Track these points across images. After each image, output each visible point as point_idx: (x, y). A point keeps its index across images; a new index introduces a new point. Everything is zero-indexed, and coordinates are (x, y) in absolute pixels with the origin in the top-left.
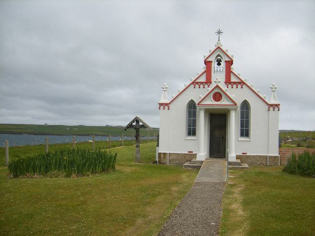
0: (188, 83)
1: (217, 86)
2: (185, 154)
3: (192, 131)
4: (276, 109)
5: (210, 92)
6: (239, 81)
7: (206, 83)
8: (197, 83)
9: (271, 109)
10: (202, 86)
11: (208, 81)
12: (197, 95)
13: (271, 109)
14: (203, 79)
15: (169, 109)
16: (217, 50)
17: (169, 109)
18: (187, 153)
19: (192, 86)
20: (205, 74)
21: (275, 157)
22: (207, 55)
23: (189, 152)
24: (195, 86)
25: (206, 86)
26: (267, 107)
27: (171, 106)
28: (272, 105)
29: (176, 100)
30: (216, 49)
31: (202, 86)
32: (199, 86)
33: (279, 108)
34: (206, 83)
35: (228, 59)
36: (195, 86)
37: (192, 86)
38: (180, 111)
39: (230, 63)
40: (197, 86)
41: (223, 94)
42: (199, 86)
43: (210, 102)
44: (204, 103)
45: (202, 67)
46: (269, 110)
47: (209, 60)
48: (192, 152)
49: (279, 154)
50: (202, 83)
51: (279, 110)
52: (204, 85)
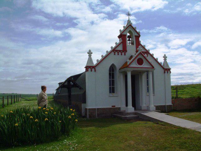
0: (109, 50)
1: (140, 53)
2: (110, 108)
3: (112, 90)
4: (169, 72)
5: (135, 58)
6: (145, 51)
7: (123, 51)
8: (117, 51)
9: (166, 72)
10: (120, 53)
11: (125, 50)
12: (118, 61)
13: (166, 72)
14: (120, 48)
15: (95, 71)
16: (129, 27)
17: (95, 71)
18: (111, 107)
19: (113, 53)
20: (122, 44)
21: (170, 106)
22: (122, 29)
23: (112, 106)
24: (115, 53)
25: (123, 53)
26: (163, 71)
27: (97, 68)
28: (166, 69)
29: (101, 64)
30: (129, 26)
31: (120, 53)
32: (118, 53)
33: (170, 71)
34: (123, 51)
35: (136, 34)
36: (115, 53)
37: (113, 53)
38: (104, 72)
39: (138, 36)
40: (116, 53)
41: (144, 60)
42: (118, 53)
43: (135, 65)
44: (131, 66)
45: (118, 41)
46: (165, 73)
47: (124, 33)
48: (115, 106)
49: (172, 103)
50: (120, 51)
51: (170, 73)
52: (121, 53)
